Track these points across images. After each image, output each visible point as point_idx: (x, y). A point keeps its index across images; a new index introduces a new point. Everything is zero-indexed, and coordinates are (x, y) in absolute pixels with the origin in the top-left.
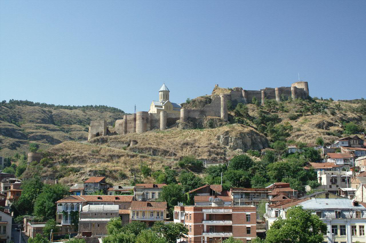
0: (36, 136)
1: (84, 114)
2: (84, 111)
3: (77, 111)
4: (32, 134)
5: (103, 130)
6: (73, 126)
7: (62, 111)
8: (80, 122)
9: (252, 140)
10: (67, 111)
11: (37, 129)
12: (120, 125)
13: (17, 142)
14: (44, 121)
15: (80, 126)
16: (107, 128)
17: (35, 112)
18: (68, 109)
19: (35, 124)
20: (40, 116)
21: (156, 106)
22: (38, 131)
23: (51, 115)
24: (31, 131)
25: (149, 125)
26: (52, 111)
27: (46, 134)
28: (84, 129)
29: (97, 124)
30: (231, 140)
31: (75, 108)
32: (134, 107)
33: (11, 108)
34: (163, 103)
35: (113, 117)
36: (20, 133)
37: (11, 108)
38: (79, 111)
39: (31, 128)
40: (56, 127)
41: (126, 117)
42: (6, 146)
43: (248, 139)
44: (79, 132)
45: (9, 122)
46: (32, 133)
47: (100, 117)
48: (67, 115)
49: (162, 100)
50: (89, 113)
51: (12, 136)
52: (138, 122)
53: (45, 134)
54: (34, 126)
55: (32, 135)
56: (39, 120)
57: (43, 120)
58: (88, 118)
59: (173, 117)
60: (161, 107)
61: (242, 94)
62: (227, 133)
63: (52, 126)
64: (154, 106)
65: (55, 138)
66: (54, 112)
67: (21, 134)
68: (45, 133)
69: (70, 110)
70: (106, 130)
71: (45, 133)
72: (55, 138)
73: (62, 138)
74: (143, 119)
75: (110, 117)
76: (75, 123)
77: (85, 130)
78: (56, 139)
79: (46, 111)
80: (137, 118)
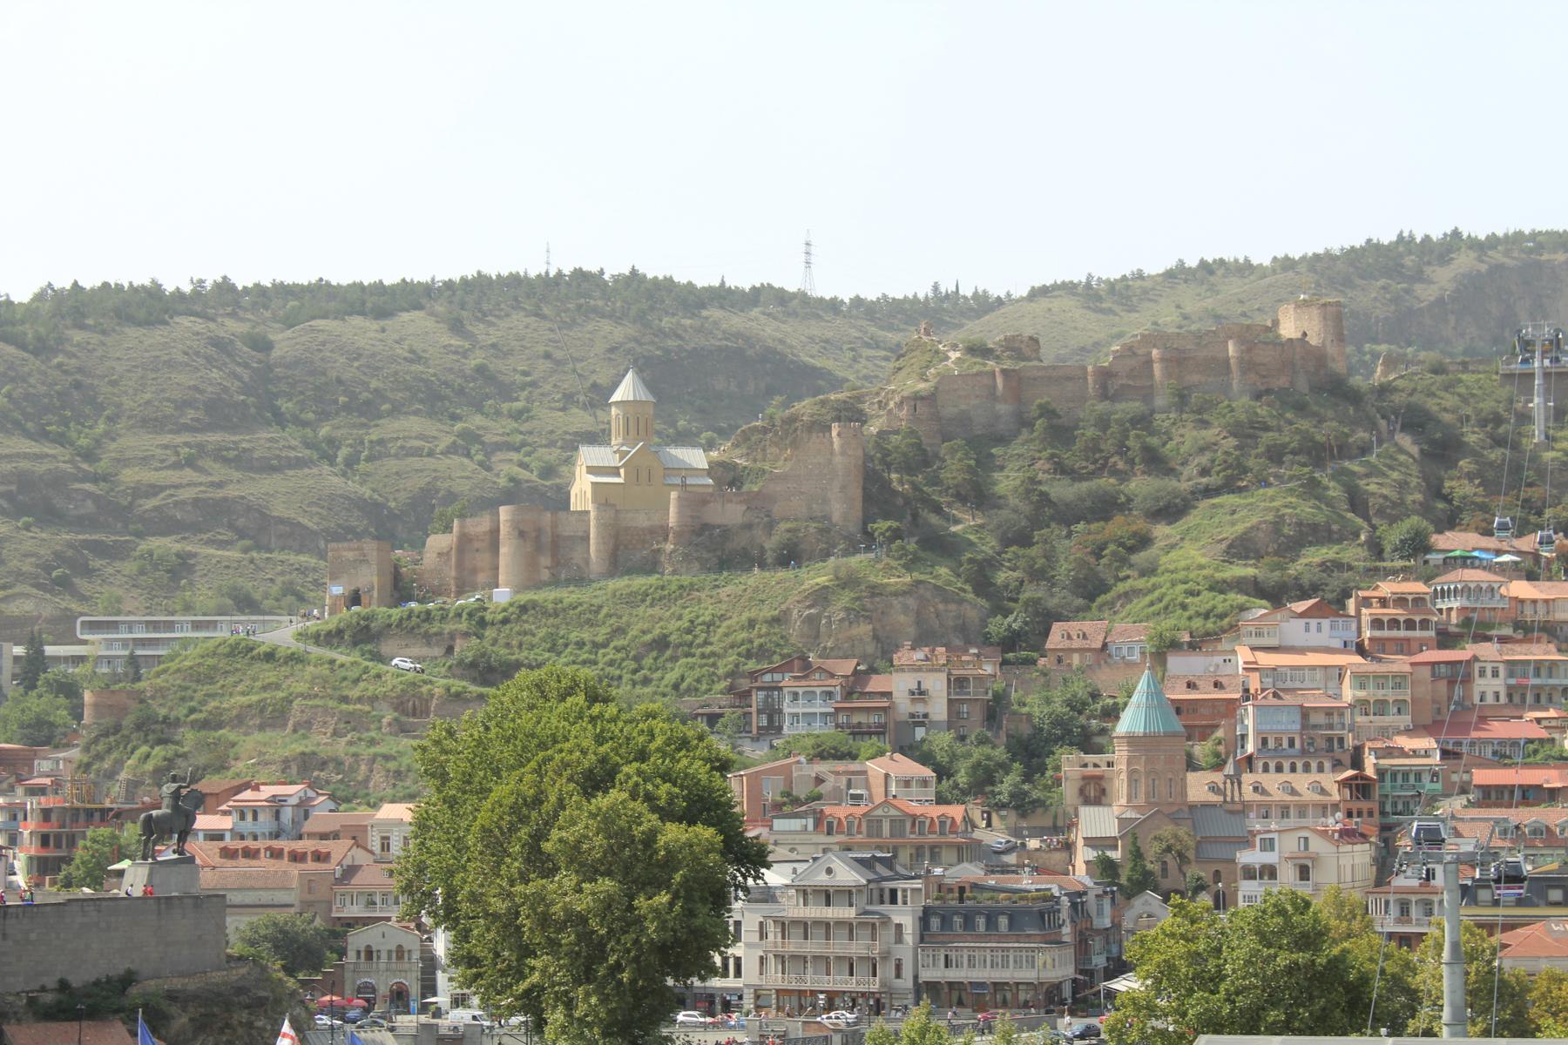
0: (176, 504)
1: (455, 342)
2: (457, 327)
3: (412, 322)
4: (155, 494)
5: (375, 579)
6: (390, 427)
7: (321, 337)
8: (434, 398)
10: (361, 331)
11: (177, 466)
12: (440, 555)
13: (70, 545)
14: (219, 413)
15: (430, 427)
16: (396, 568)
17: (170, 364)
18: (362, 313)
19: (167, 439)
20: (196, 388)
21: (592, 470)
22: (185, 482)
23: (260, 362)
24: (149, 476)
25: (545, 561)
26: (271, 337)
27: (232, 491)
28: (446, 441)
29: (350, 555)
30: (830, 623)
31: (411, 296)
32: (803, 248)
33: (41, 348)
34: (623, 455)
35: (629, 351)
36: (89, 495)
37: (41, 348)
38: (430, 323)
39: (145, 461)
40: (289, 440)
41: (462, 526)
42: (19, 576)
43: (902, 618)
44: (415, 462)
45: (28, 434)
46: (154, 490)
47: (548, 356)
48: (356, 359)
49: (620, 440)
50: (487, 334)
51: (50, 516)
52: (503, 550)
53: (220, 494)
54: (166, 447)
55: (150, 504)
56: (191, 414)
57: (212, 406)
58: (481, 370)
59: (642, 521)
60: (615, 471)
61: (995, 386)
62: (821, 597)
63: (262, 440)
64: (584, 469)
65: (279, 509)
66: (285, 343)
67: (96, 499)
68: (220, 485)
69: (375, 325)
70: (389, 579)
71: (220, 485)
72: (275, 514)
73: (315, 509)
75: (612, 350)
76: (397, 410)
77: (452, 450)
78: (281, 521)
79: (239, 344)
80: (504, 530)
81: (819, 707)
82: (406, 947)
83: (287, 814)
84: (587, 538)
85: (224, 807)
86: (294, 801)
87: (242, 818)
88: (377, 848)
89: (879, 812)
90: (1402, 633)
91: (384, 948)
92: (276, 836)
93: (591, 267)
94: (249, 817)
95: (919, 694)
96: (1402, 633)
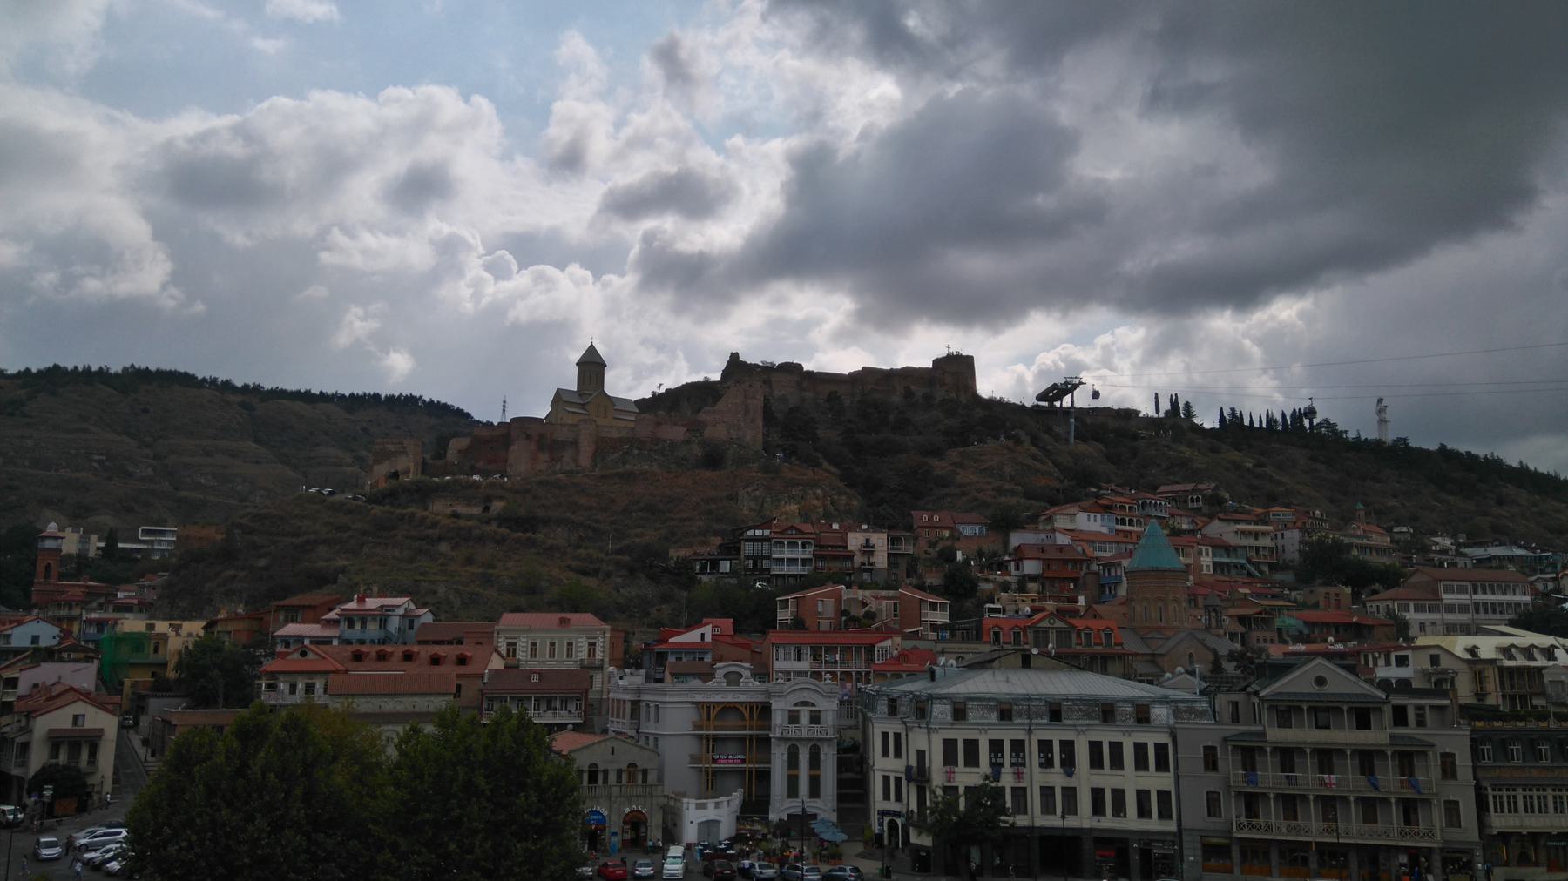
9: (825, 507)
74: (528, 437)
81: (799, 554)
82: (640, 766)
83: (394, 624)
84: (575, 444)
85: (332, 615)
86: (401, 611)
87: (351, 625)
88: (503, 649)
89: (1045, 624)
90: (1127, 528)
91: (612, 768)
92: (383, 642)
93: (417, 394)
94: (358, 626)
95: (868, 549)
96: (1127, 528)
